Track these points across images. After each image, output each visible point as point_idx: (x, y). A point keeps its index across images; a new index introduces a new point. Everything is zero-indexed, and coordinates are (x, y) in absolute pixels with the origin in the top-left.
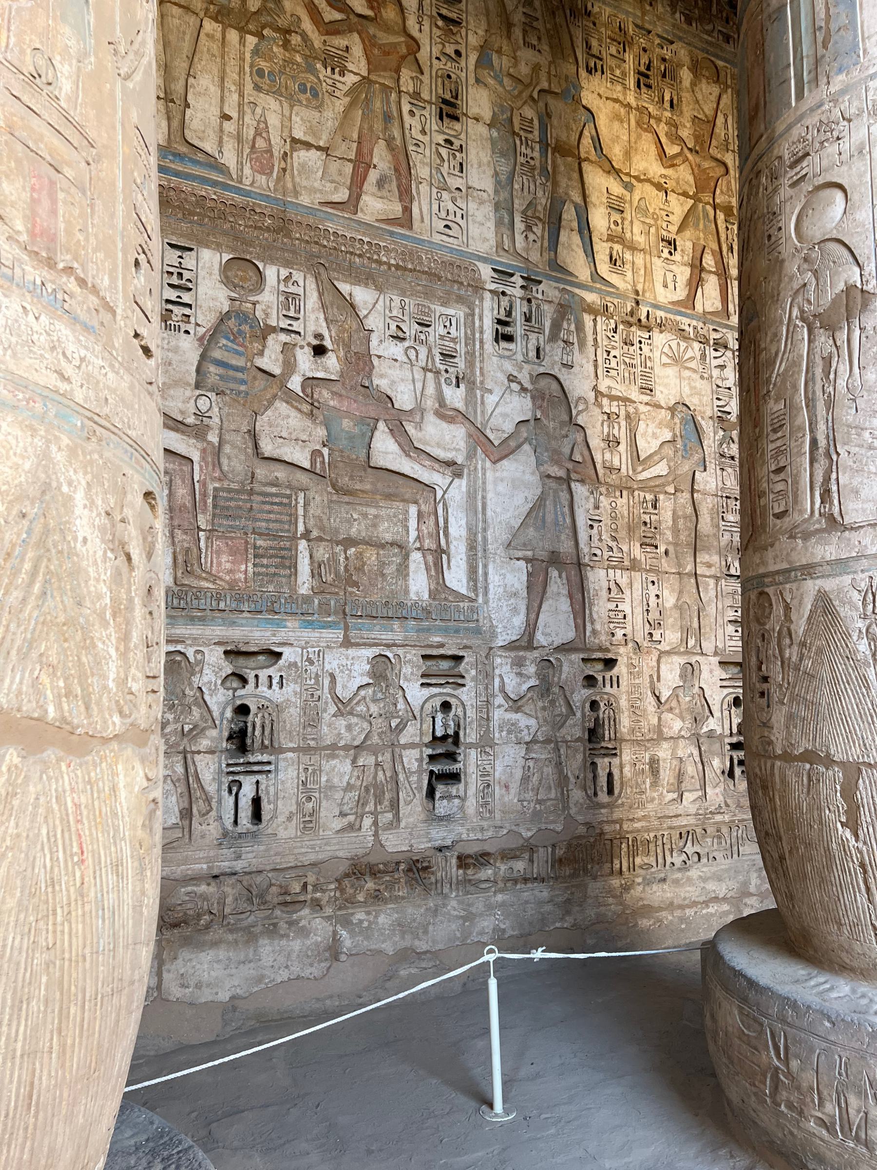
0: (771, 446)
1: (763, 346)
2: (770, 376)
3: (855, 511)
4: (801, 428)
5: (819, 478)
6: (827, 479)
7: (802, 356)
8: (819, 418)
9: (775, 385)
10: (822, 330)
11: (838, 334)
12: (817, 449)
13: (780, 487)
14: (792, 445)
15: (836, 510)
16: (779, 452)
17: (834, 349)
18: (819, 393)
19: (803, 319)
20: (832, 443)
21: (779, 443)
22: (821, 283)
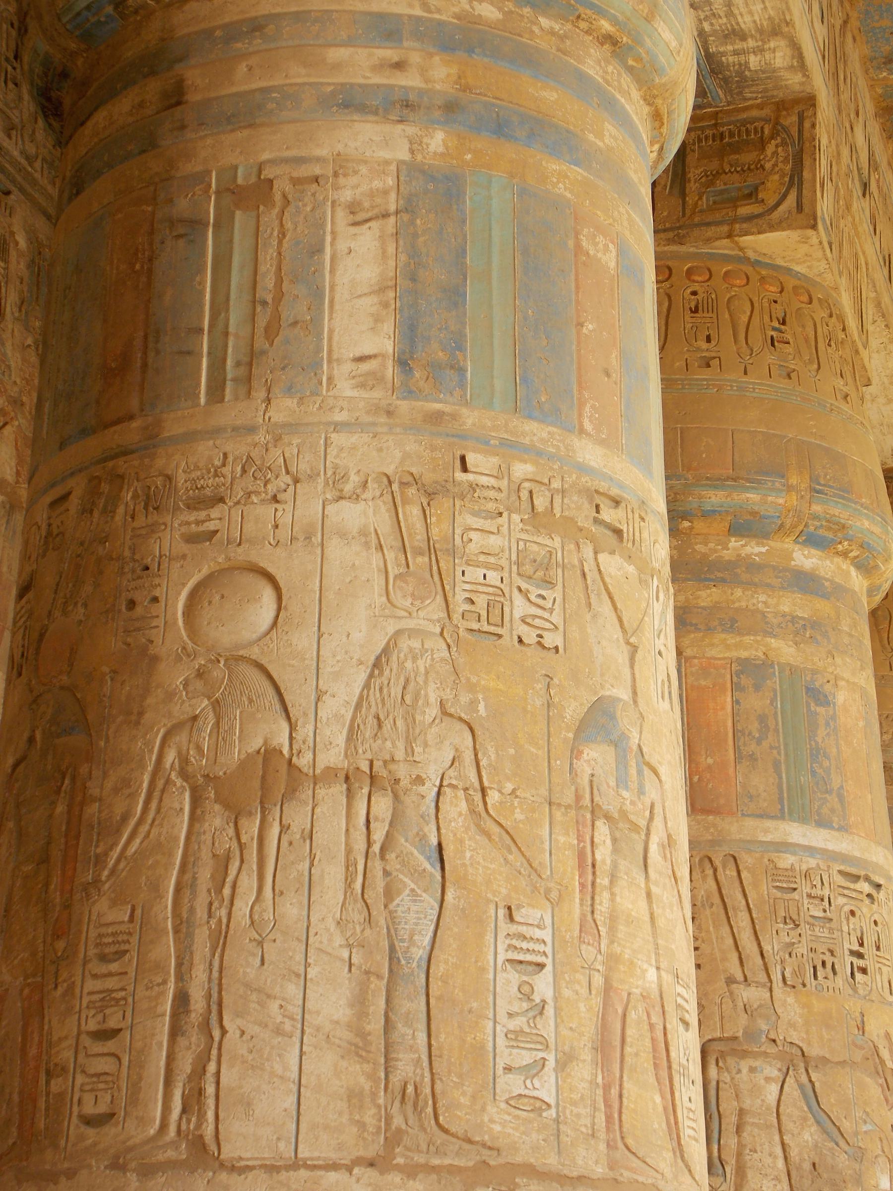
0: (91, 985)
1: (95, 791)
2: (106, 854)
3: (242, 1138)
4: (160, 967)
5: (185, 1065)
6: (199, 1071)
7: (176, 839)
8: (197, 958)
9: (113, 872)
10: (217, 807)
11: (243, 822)
12: (188, 1012)
13: (104, 1065)
14: (141, 993)
15: (208, 1130)
16: (108, 1000)
17: (235, 845)
18: (201, 913)
19: (184, 774)
20: (214, 1008)
21: (111, 983)
22: (224, 726)
